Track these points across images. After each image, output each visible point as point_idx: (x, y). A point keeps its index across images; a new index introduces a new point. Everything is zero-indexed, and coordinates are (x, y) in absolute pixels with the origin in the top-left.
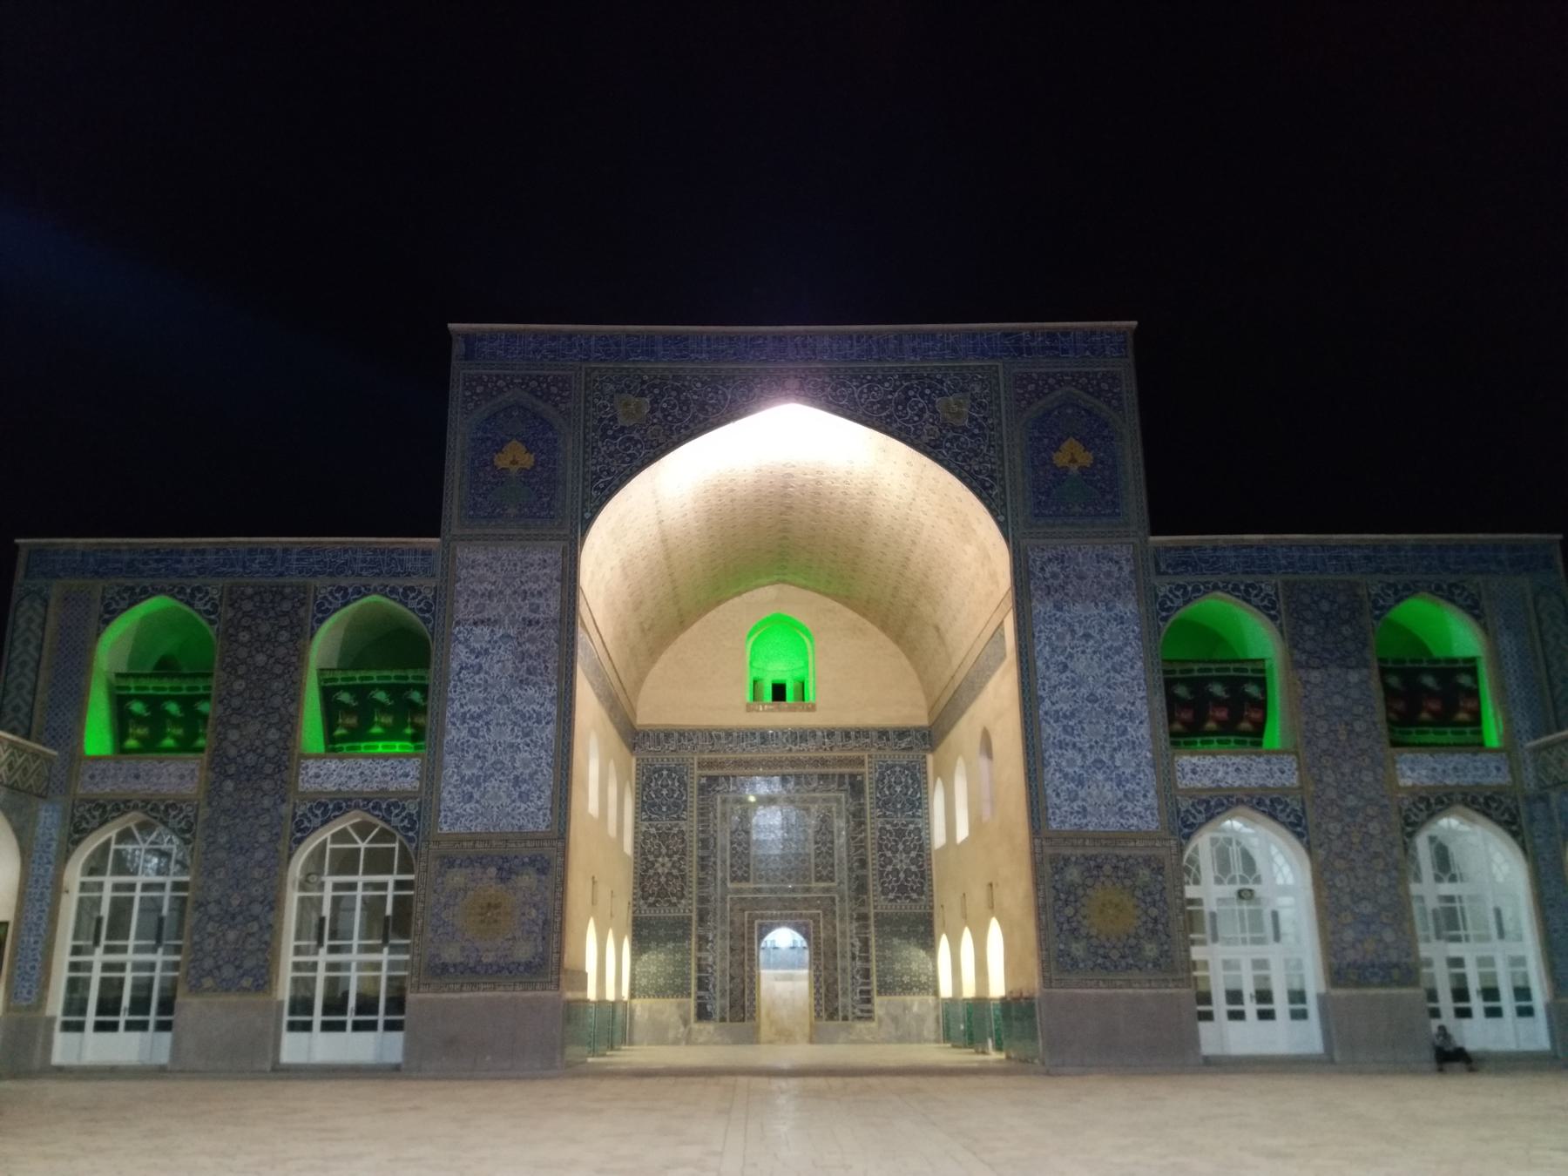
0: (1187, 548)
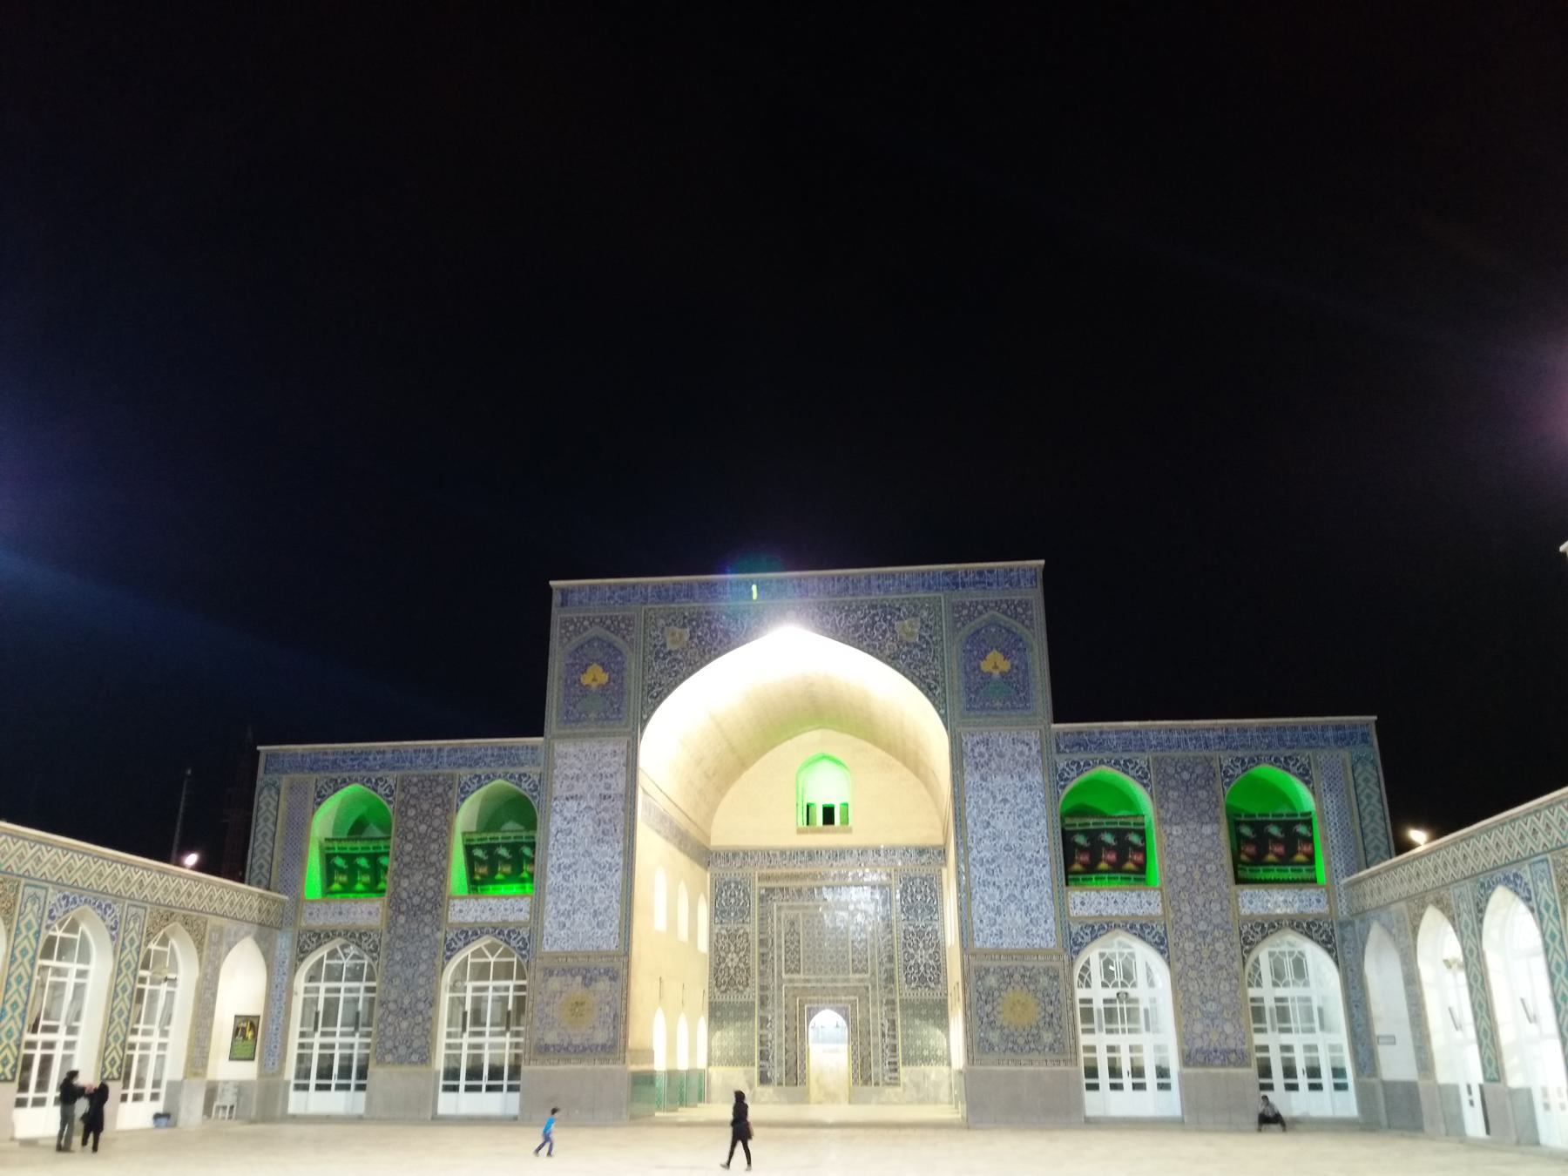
0: (1080, 733)
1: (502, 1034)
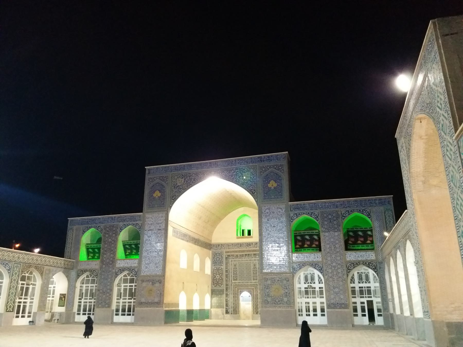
0: (297, 205)
1: (131, 299)
